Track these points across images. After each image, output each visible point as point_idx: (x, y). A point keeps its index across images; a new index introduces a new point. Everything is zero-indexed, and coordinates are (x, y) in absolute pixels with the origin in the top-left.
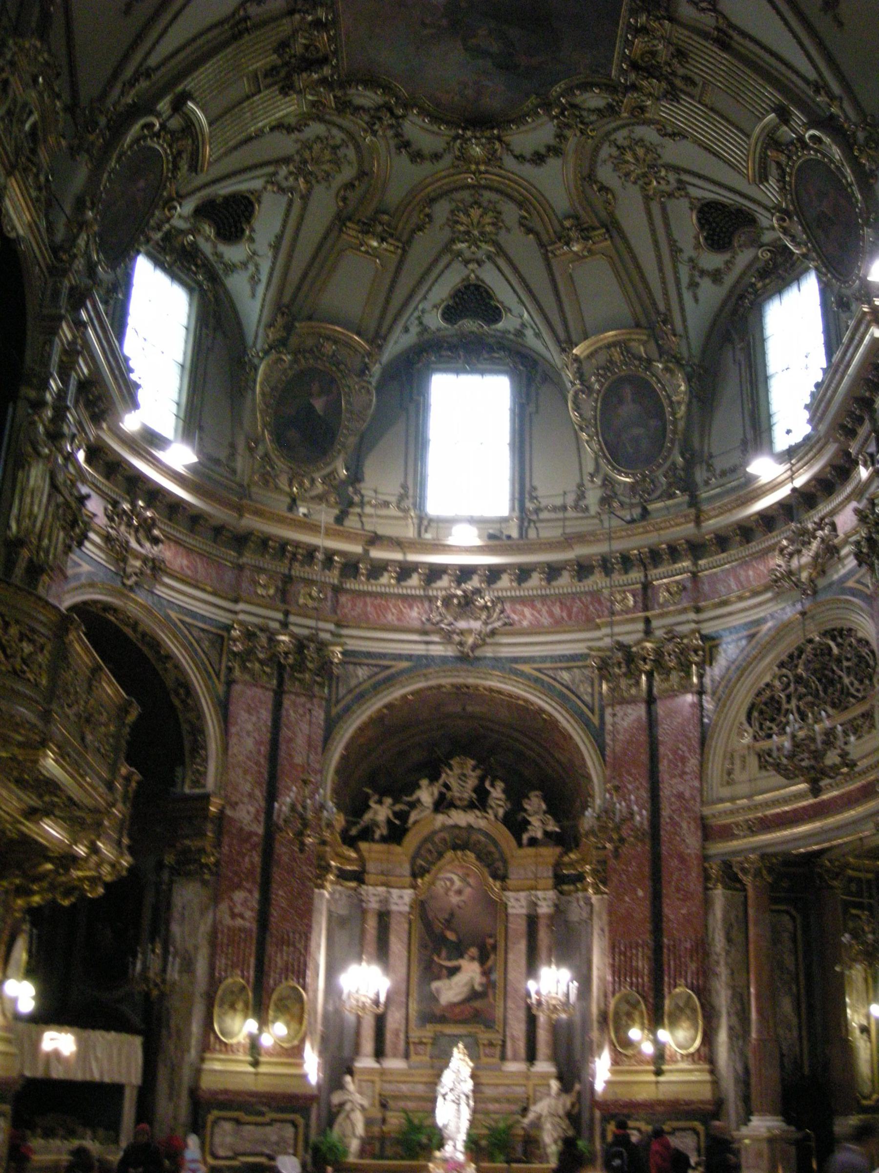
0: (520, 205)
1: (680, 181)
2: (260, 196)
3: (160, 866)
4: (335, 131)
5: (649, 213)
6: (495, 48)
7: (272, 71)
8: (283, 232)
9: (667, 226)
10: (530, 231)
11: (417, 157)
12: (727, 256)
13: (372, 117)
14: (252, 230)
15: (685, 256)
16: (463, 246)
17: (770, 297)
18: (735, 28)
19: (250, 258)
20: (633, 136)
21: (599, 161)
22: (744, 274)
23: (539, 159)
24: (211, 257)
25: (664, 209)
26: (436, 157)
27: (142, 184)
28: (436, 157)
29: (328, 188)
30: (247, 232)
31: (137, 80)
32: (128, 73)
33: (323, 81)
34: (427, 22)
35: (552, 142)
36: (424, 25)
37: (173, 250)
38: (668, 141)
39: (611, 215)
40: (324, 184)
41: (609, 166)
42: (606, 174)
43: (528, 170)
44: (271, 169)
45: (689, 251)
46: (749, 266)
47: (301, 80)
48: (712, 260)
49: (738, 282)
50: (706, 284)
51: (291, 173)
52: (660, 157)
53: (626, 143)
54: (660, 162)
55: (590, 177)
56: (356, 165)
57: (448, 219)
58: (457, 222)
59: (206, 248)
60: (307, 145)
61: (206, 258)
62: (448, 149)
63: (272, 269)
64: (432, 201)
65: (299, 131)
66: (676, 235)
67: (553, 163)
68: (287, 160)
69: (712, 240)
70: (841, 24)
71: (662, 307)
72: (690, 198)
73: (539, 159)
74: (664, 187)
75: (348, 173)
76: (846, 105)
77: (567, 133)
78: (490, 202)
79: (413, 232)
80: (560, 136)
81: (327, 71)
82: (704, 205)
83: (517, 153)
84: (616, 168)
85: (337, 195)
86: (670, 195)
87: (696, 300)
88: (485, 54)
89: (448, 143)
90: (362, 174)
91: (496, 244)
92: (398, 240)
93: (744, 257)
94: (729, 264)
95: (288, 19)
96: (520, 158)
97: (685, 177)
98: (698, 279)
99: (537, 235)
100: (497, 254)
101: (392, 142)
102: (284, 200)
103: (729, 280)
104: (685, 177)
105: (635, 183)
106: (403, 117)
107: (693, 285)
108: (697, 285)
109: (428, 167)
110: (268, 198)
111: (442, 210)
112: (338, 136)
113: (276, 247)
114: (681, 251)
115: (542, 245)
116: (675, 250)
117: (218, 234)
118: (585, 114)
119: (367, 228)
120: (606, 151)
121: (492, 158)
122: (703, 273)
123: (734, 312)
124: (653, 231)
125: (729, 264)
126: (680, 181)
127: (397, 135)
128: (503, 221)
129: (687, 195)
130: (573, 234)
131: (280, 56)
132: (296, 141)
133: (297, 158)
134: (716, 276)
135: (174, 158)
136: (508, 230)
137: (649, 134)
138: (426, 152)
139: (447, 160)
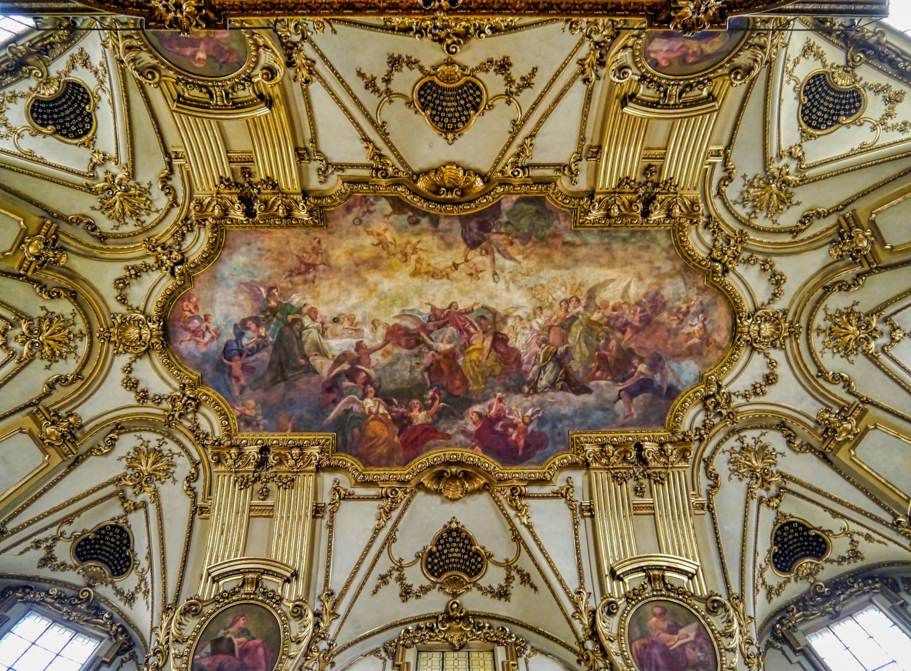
0: (78, 375)
1: (144, 505)
2: (88, 147)
3: (270, 72)
4: (155, 216)
5: (102, 486)
6: (248, 341)
7: (247, 173)
8: (45, 164)
9: (95, 503)
10: (51, 386)
11: (122, 284)
12: (71, 561)
13: (170, 247)
14: (45, 135)
15: (65, 528)
16: (24, 327)
17: (44, 615)
18: (332, 518)
19: (12, 130)
20: (176, 456)
21: (138, 434)
22: (56, 582)
23: (132, 384)
24: (11, 89)
25: (110, 496)
26: (123, 300)
27: (201, 55)
28: (123, 300)
29: (93, 208)
30: (44, 130)
31: (310, 73)
32: (320, 66)
33: (225, 211)
34: (275, 291)
35: (151, 395)
36: (270, 290)
37: (29, 54)
38: (182, 485)
39: (89, 452)
40: (98, 205)
41: (138, 443)
42: (127, 443)
43: (117, 375)
44: (124, 158)
45: (68, 529)
46: (66, 584)
47: (231, 196)
48: (64, 552)
49: (46, 580)
50: (41, 553)
51: (114, 176)
52: (163, 483)
53: (165, 453)
54: (158, 484)
55: (120, 428)
56: (115, 231)
57: (53, 313)
58: (51, 321)
59: (24, 86)
60: (144, 192)
61: (7, 85)
62: (131, 309)
63: (8, 153)
64: (73, 296)
65: (163, 187)
66: (83, 515)
67: (130, 398)
68: (132, 175)
69: (85, 545)
70: (375, 592)
71: (10, 526)
72: (126, 515)
73: (132, 384)
74: (129, 492)
75: (106, 225)
76: (336, 623)
77: (166, 405)
78: (76, 347)
79: (38, 282)
80: (158, 400)
81: (237, 213)
82: (121, 529)
83: (134, 365)
84: (136, 450)
85: (84, 216)
86: (124, 499)
87: (22, 553)
88: (240, 335)
89: (138, 308)
90: (103, 238)
91: (31, 359)
92: (35, 270)
93: (74, 577)
94: (63, 566)
95: (299, 191)
96: (128, 369)
97: (152, 508)
98: (43, 546)
99: (47, 395)
100: (20, 362)
101: (138, 263)
102: (84, 169)
103: (46, 573)
104: (152, 508)
105: (129, 467)
106: (173, 273)
107: (37, 544)
108: (38, 547)
109: (109, 292)
110: (86, 153)
111: (64, 307)
112: (149, 220)
113: (30, 156)
114: (71, 523)
115: (40, 399)
116: (68, 520)
117: (38, 100)
118: (190, 416)
119: (53, 243)
120: (153, 439)
121: (126, 345)
122: (50, 548)
123: (16, 589)
124: (88, 493)
125: (63, 566)
126: (144, 505)
127: (148, 268)
128: (57, 361)
129: (127, 512)
130: (64, 425)
131: (263, 182)
132: (150, 184)
133: (132, 183)
134: (46, 561)
135: (206, 87)
136: (48, 368)
137: (183, 467)
138: (127, 291)
139: (122, 309)
